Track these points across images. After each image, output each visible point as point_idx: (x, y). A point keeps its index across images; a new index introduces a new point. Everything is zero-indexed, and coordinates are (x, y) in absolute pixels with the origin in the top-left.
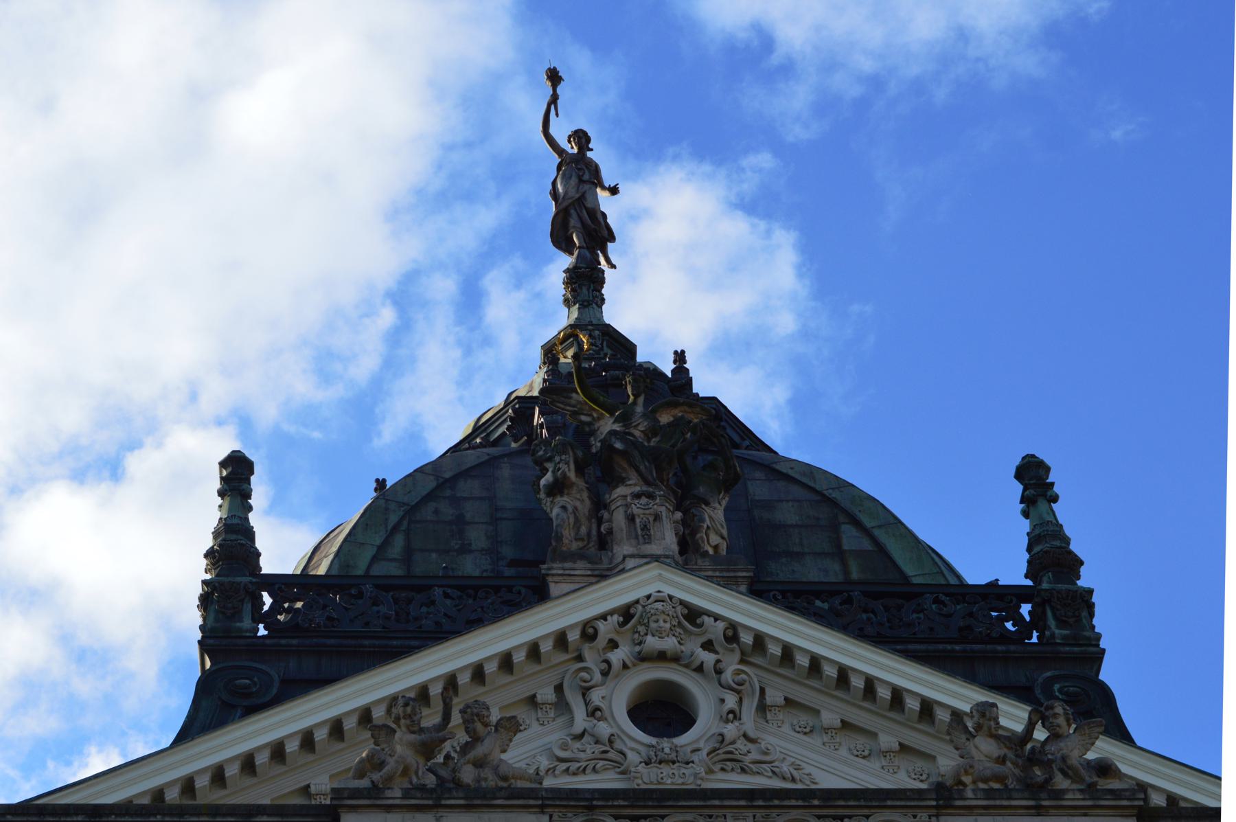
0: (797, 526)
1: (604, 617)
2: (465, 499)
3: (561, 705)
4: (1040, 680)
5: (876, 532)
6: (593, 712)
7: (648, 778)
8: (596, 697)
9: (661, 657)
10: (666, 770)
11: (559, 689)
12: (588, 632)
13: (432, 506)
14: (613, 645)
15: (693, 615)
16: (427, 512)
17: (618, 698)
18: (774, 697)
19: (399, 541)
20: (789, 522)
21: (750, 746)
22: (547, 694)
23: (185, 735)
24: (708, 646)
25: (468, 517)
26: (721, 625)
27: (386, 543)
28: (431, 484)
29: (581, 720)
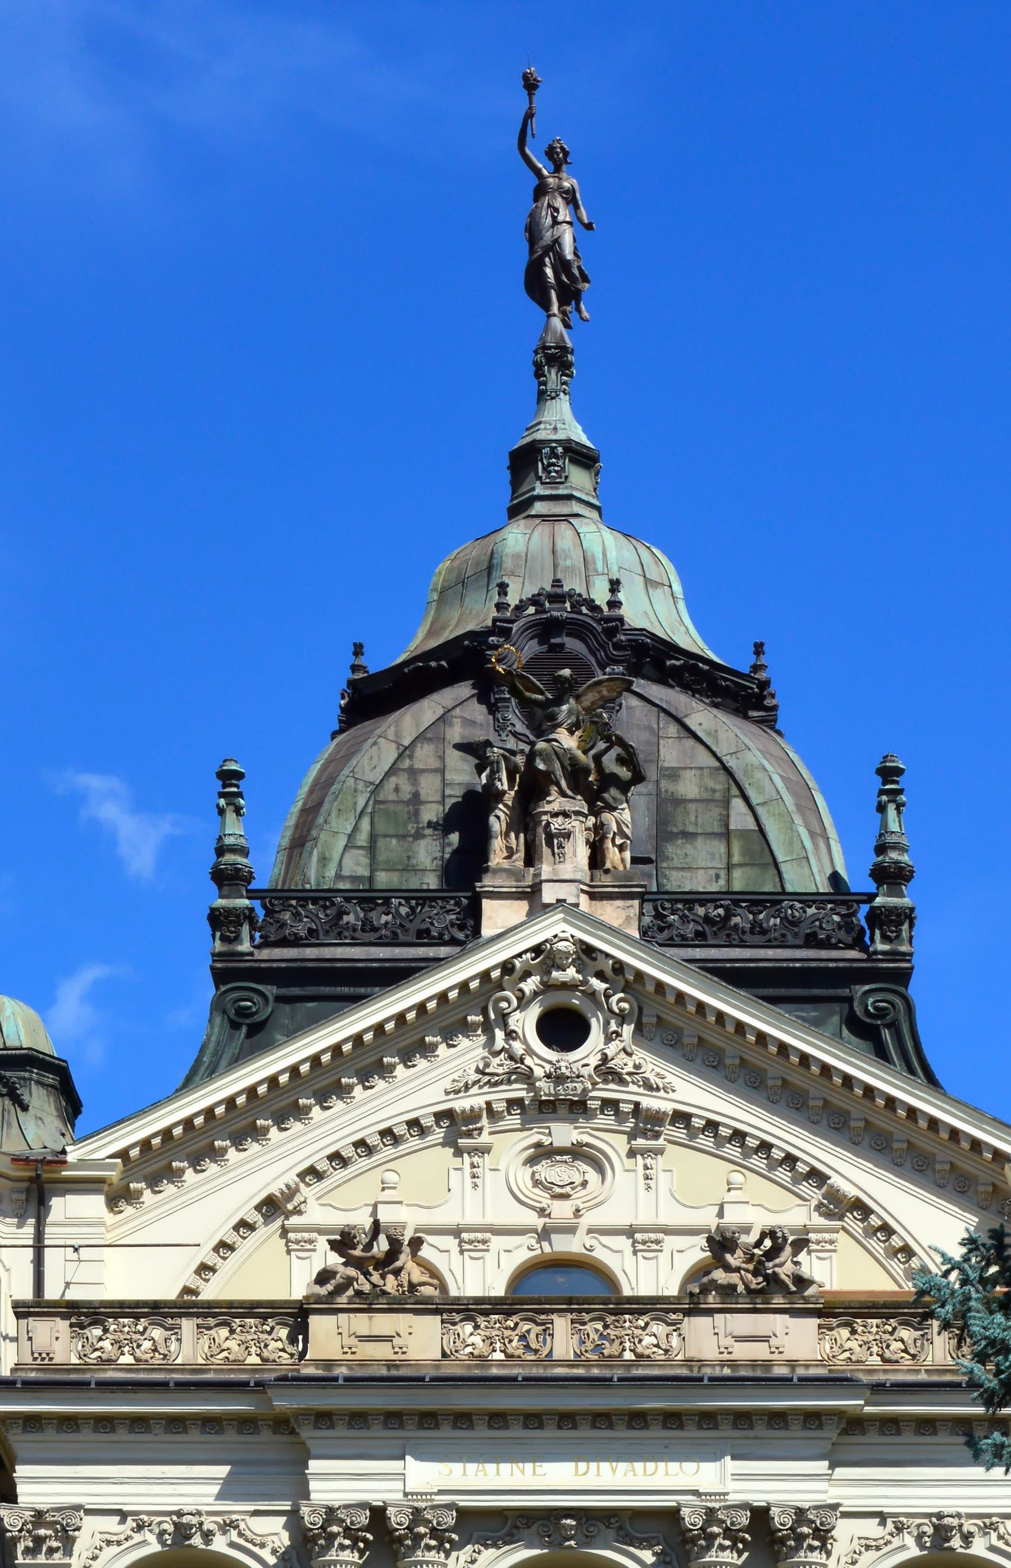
1: (520, 955)
2: (423, 771)
4: (859, 993)
5: (761, 811)
6: (510, 1035)
9: (565, 986)
12: (507, 967)
13: (393, 780)
14: (526, 975)
16: (387, 793)
17: (526, 1022)
19: (365, 825)
20: (690, 796)
24: (600, 975)
25: (423, 793)
27: (356, 829)
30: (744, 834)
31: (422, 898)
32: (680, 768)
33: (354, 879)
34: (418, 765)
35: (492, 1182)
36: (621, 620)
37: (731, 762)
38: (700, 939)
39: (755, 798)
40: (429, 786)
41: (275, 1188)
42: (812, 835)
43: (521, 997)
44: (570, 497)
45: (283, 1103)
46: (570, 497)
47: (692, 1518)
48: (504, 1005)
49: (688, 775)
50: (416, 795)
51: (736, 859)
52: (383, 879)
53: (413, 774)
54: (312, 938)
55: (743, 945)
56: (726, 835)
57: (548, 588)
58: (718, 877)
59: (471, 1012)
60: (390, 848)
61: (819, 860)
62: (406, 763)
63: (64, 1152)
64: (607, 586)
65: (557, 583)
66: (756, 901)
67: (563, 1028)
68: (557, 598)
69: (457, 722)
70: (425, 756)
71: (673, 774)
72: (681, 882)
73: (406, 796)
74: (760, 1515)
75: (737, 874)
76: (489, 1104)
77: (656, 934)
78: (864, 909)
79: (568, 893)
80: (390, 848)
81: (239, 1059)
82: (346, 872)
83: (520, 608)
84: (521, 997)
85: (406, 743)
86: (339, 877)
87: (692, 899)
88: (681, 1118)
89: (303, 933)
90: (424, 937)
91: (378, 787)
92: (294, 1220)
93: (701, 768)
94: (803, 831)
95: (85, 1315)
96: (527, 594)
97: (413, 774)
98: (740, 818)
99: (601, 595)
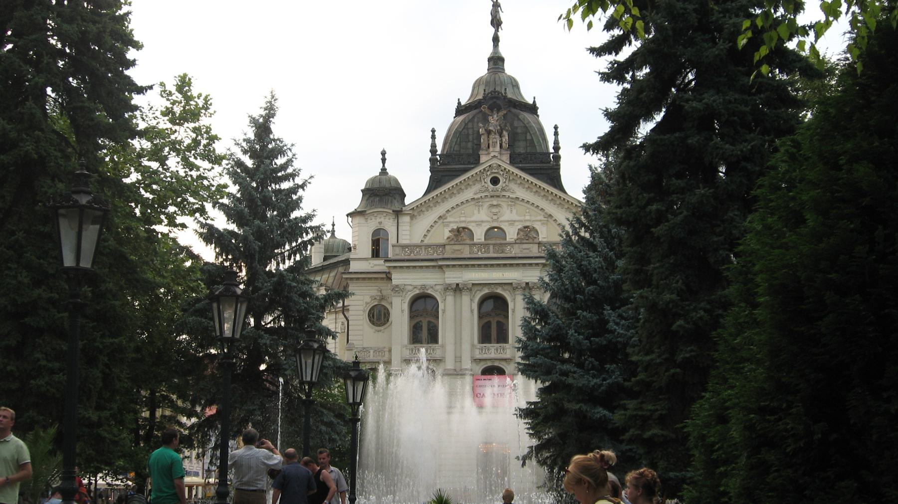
31: (469, 155)
35: (481, 211)
40: (471, 132)
45: (443, 198)
47: (514, 285)
52: (462, 151)
54: (449, 163)
56: (526, 140)
67: (495, 181)
68: (495, 91)
70: (470, 125)
71: (517, 128)
72: (518, 150)
74: (527, 284)
77: (513, 162)
81: (436, 188)
87: (520, 154)
90: (469, 163)
97: (468, 129)
98: (529, 137)
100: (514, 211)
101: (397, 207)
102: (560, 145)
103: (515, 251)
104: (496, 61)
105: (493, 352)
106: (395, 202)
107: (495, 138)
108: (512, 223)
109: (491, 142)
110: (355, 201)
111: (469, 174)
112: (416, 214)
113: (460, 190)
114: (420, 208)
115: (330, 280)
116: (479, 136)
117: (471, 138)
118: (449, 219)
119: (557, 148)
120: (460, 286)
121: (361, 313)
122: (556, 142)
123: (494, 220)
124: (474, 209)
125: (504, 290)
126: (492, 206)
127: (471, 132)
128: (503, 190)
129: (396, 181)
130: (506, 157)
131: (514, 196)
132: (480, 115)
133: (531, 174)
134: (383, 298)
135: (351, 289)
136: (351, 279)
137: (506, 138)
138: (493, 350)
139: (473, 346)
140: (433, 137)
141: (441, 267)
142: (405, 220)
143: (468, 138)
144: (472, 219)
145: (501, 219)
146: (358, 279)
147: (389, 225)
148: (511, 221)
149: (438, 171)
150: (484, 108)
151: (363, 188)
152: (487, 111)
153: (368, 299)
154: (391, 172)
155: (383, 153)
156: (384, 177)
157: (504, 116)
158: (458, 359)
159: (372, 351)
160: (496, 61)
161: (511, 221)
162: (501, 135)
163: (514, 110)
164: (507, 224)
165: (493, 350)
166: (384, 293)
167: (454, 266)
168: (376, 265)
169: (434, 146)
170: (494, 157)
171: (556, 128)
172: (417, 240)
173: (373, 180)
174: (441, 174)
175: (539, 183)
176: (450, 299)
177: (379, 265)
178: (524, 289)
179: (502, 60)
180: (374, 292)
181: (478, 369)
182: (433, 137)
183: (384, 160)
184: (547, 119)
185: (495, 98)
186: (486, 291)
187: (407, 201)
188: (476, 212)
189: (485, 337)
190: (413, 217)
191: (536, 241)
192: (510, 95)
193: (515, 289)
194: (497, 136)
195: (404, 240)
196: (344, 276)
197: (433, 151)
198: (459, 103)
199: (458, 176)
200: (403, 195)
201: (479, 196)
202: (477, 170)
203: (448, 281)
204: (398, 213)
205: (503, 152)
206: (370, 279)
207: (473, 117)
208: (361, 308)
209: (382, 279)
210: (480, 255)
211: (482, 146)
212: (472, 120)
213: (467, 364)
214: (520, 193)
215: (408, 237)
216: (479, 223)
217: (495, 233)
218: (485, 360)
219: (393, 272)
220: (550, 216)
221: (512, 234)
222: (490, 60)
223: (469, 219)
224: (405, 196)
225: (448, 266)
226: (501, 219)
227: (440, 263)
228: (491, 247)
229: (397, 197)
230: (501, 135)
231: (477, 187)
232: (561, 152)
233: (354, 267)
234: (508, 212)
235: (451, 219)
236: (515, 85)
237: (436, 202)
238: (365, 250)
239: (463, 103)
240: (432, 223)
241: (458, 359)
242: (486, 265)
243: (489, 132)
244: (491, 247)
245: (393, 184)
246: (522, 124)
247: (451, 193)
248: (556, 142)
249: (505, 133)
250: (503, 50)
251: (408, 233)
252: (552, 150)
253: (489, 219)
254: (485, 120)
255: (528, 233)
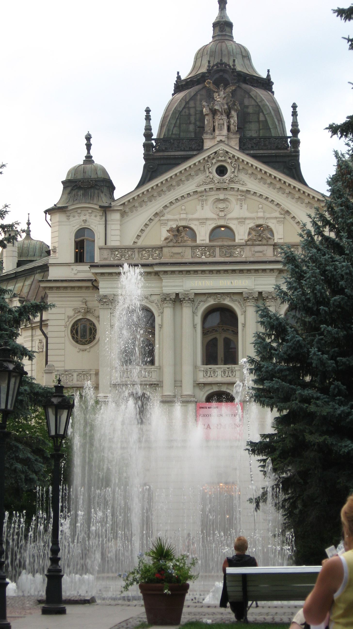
0: (252, 113)
1: (212, 154)
2: (191, 107)
3: (204, 170)
5: (266, 115)
7: (219, 186)
8: (210, 169)
9: (222, 161)
10: (222, 184)
11: (204, 167)
12: (209, 157)
13: (184, 110)
14: (214, 158)
15: (227, 152)
16: (183, 113)
17: (214, 169)
18: (241, 167)
19: (178, 121)
21: (236, 178)
22: (202, 168)
23: (142, 183)
24: (229, 158)
26: (232, 155)
27: (176, 122)
28: (184, 104)
29: (208, 174)
30: (262, 121)
31: (191, 140)
32: (248, 106)
33: (175, 134)
34: (190, 106)
35: (205, 207)
36: (235, 69)
37: (260, 104)
38: (252, 148)
39: (265, 113)
40: (192, 111)
41: (158, 211)
42: (278, 120)
43: (212, 164)
44: (226, 35)
45: (159, 191)
46: (226, 35)
48: (208, 166)
49: (250, 107)
50: (189, 113)
51: (261, 128)
52: (182, 135)
53: (189, 108)
54: (166, 150)
55: (262, 149)
56: (259, 122)
57: (219, 61)
58: (257, 132)
59: (200, 169)
60: (184, 126)
61: (280, 127)
62: (187, 106)
63: (111, 204)
64: (232, 61)
65: (221, 60)
66: (265, 138)
67: (222, 171)
68: (221, 64)
69: (199, 95)
70: (192, 104)
71: (247, 107)
73: (187, 114)
74: (260, 293)
75: (261, 131)
76: (205, 189)
77: (243, 148)
78: (289, 140)
79: (223, 139)
80: (184, 126)
81: (150, 179)
82: (174, 133)
83: (213, 67)
84: (212, 164)
85: (187, 100)
86: (172, 134)
87: (251, 139)
88: (248, 191)
89: (164, 149)
90: (191, 149)
91: (181, 112)
92: (162, 218)
93: (253, 105)
94: (276, 120)
95: (113, 249)
96: (215, 63)
97: (189, 108)
98: (262, 118)
99: (231, 64)
100: (245, 207)
101: (105, 202)
102: (299, 127)
103: (247, 254)
104: (223, 27)
105: (219, 374)
106: (102, 195)
107: (221, 119)
108: (242, 220)
109: (216, 124)
110: (55, 195)
111: (190, 163)
112: (127, 210)
113: (180, 182)
114: (133, 203)
115: (26, 290)
116: (202, 117)
117: (192, 119)
118: (167, 216)
119: (295, 131)
120: (181, 296)
121: (63, 329)
122: (295, 124)
123: (220, 218)
124: (196, 205)
125: (233, 301)
126: (218, 200)
127: (192, 111)
128: (231, 181)
129: (104, 171)
130: (235, 142)
131: (244, 189)
132: (204, 92)
133: (265, 163)
134: (88, 311)
135: (50, 300)
136: (51, 288)
137: (234, 119)
138: (219, 372)
139: (195, 367)
140: (148, 118)
141: (157, 273)
142: (115, 217)
143: (189, 119)
144: (196, 216)
145: (229, 216)
146: (58, 288)
147: (95, 224)
148: (241, 218)
149: (154, 159)
150: (209, 83)
151: (64, 179)
152: (212, 87)
153: (70, 312)
154: (98, 160)
155: (88, 138)
156: (89, 166)
157: (233, 93)
158: (178, 383)
159: (75, 375)
160: (223, 27)
161: (241, 218)
162: (228, 116)
163: (244, 86)
164: (236, 222)
165: (219, 372)
166: (90, 305)
167: (173, 272)
168: (79, 272)
169: (148, 129)
170: (220, 142)
171: (294, 106)
172: (129, 242)
173: (75, 170)
174: (157, 162)
175: (274, 173)
176: (168, 312)
177: (83, 271)
178: (257, 300)
179: (230, 25)
180: (78, 304)
181: (202, 395)
182: (148, 118)
183: (89, 146)
184: (283, 96)
185: (221, 71)
186: (211, 302)
187: (117, 195)
188: (199, 207)
189: (210, 357)
190: (123, 214)
191: (271, 242)
192: (239, 68)
193: (246, 299)
194: (224, 117)
195: (113, 242)
196: (43, 285)
197: (148, 135)
198: (179, 77)
199: (178, 164)
200: (111, 188)
201: (202, 189)
202: (200, 157)
203: (166, 290)
204: (106, 210)
205: (231, 135)
206: (73, 288)
207: (196, 95)
208: (63, 323)
209: (87, 288)
210: (204, 259)
211: (206, 129)
212: (193, 98)
213: (188, 389)
214: (252, 185)
215: (118, 238)
216: (203, 221)
217: (221, 232)
218: (210, 384)
219: (99, 278)
220: (288, 212)
221: (241, 234)
222: (215, 25)
223: (190, 216)
224: (114, 188)
225: (165, 272)
226: (229, 216)
227: (157, 269)
228: (217, 250)
229: (105, 189)
230: (228, 116)
231: (201, 178)
232: (300, 136)
233: (54, 273)
234: (237, 207)
235: (167, 216)
236: (245, 55)
237: (151, 196)
238: (67, 253)
239: (183, 77)
240: (146, 221)
241: (178, 383)
242: (211, 272)
243: (214, 112)
244: (217, 250)
245: (100, 175)
246: (253, 103)
247: (170, 185)
248: (295, 124)
249: (234, 114)
250: (231, 14)
251: (118, 233)
252: (289, 134)
253: (215, 216)
254: (210, 97)
255: (261, 233)
